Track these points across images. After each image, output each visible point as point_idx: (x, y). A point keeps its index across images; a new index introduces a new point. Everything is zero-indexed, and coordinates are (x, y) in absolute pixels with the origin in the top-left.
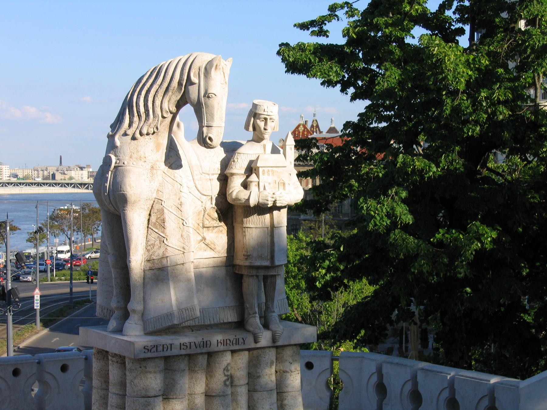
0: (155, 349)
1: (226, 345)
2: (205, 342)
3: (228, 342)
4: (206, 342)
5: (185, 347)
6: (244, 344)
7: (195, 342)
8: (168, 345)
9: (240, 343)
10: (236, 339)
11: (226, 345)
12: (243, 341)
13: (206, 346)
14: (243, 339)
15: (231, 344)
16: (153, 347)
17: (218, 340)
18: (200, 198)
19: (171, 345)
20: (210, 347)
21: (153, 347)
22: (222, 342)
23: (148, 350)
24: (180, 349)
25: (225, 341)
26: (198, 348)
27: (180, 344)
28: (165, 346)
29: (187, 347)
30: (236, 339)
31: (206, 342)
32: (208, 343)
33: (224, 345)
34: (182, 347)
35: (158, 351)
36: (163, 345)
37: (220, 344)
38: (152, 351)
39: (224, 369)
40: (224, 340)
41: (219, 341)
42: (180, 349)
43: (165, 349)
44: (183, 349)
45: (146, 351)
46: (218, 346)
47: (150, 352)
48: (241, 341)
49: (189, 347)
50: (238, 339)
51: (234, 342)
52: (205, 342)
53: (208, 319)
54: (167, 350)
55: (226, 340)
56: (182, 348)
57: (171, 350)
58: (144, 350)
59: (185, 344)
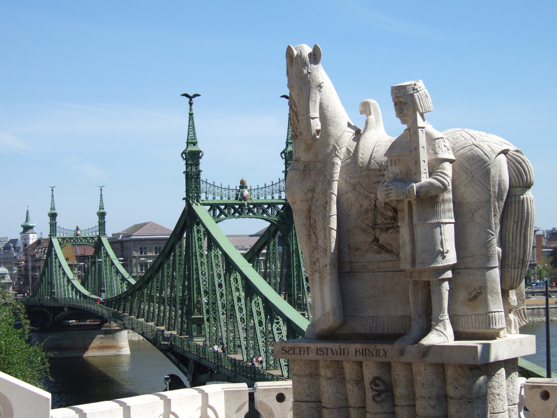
0: (292, 351)
1: (366, 356)
2: (342, 350)
3: (367, 351)
4: (344, 349)
5: (322, 353)
6: (386, 357)
7: (331, 349)
8: (305, 349)
9: (381, 355)
10: (376, 350)
11: (366, 356)
12: (384, 353)
13: (344, 355)
14: (384, 350)
15: (371, 355)
16: (290, 350)
17: (356, 349)
18: (368, 196)
19: (308, 348)
20: (347, 355)
21: (290, 350)
22: (361, 351)
23: (286, 351)
24: (317, 354)
25: (364, 350)
26: (335, 355)
27: (317, 349)
28: (302, 349)
29: (324, 352)
30: (376, 350)
31: (344, 349)
32: (346, 350)
33: (363, 355)
34: (319, 352)
35: (295, 353)
36: (300, 348)
37: (358, 354)
38: (290, 353)
39: (371, 383)
40: (363, 349)
41: (358, 350)
42: (317, 354)
43: (302, 353)
44: (320, 354)
45: (284, 352)
46: (356, 355)
47: (288, 354)
48: (382, 352)
49: (325, 353)
50: (379, 350)
51: (374, 353)
52: (342, 350)
53: (382, 327)
54: (304, 354)
55: (366, 350)
56: (319, 353)
57: (308, 354)
58: (282, 351)
59: (321, 349)
